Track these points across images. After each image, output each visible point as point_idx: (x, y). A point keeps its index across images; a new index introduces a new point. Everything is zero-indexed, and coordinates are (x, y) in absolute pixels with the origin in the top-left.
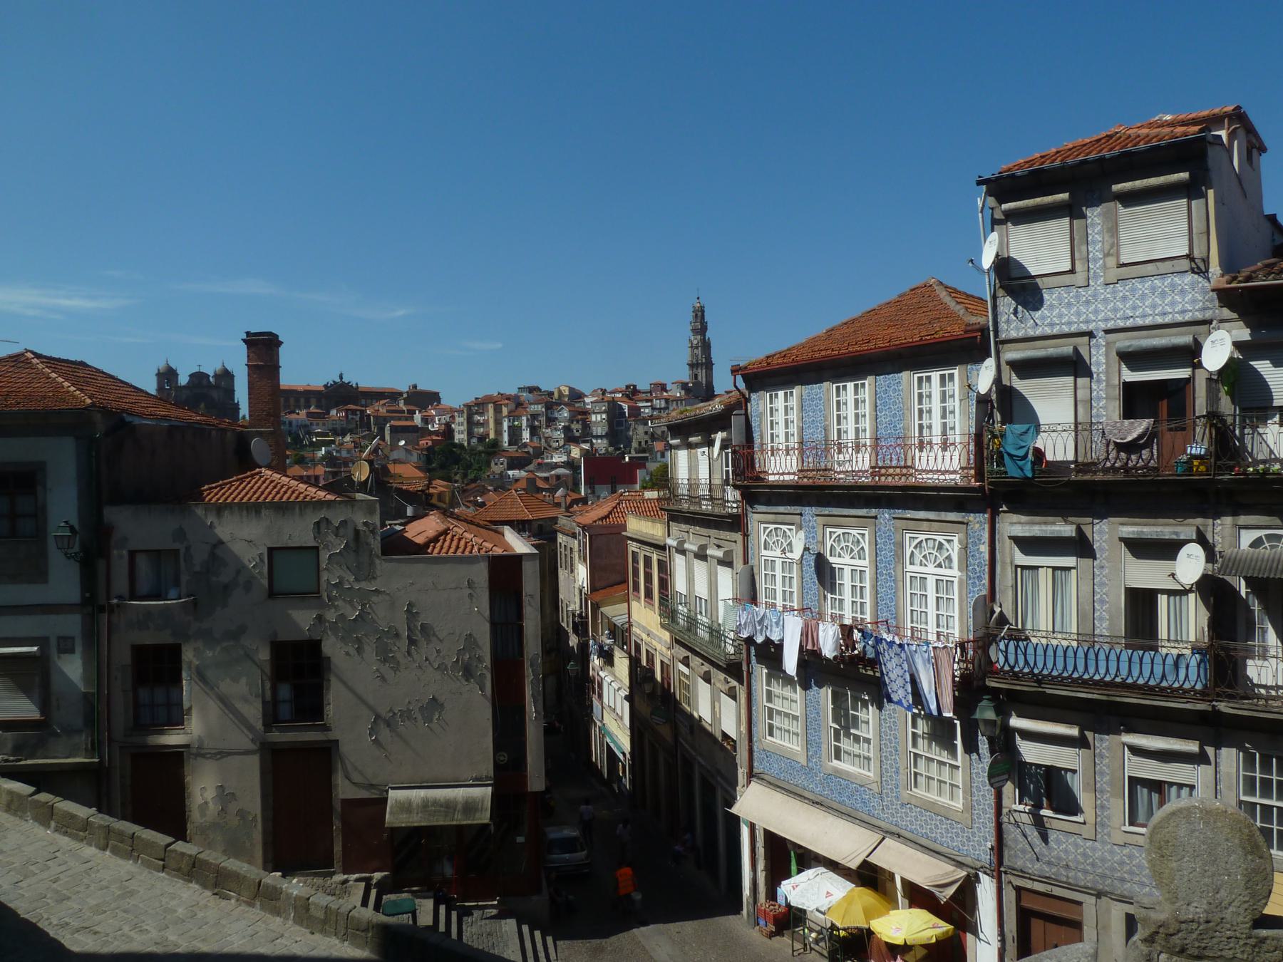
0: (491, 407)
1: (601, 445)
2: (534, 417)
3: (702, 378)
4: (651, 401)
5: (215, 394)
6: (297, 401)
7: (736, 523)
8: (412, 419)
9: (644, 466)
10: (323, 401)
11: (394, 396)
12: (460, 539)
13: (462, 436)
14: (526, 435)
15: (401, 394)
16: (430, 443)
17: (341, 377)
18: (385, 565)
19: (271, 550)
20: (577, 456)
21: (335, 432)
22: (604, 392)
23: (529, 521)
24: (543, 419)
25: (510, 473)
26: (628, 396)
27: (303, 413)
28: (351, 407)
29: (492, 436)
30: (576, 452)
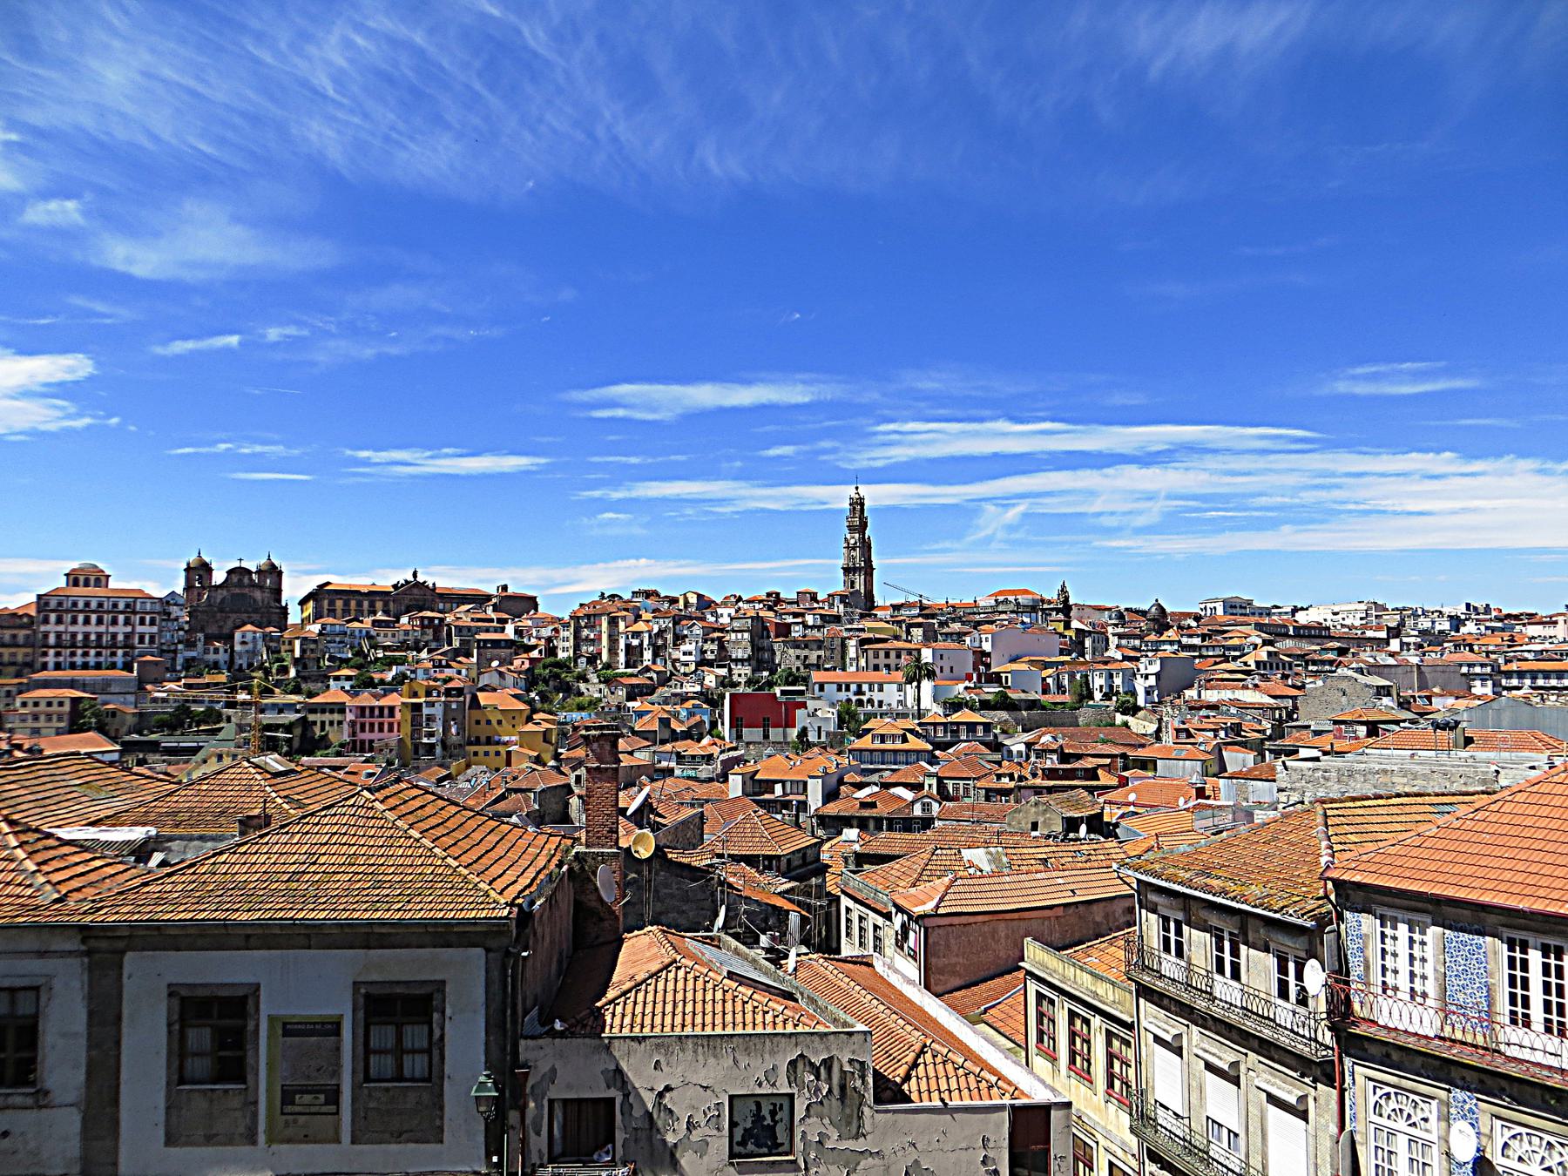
1: (742, 672)
3: (860, 585)
4: (802, 615)
5: (258, 595)
6: (360, 604)
7: (1327, 1073)
8: (503, 630)
9: (804, 705)
11: (480, 599)
12: (944, 1063)
13: (565, 655)
14: (648, 655)
15: (488, 598)
16: (527, 665)
18: (879, 1117)
19: (732, 1098)
20: (713, 685)
21: (404, 646)
22: (740, 599)
23: (778, 857)
24: (670, 637)
25: (630, 704)
26: (770, 609)
27: (368, 621)
29: (605, 657)
30: (710, 681)
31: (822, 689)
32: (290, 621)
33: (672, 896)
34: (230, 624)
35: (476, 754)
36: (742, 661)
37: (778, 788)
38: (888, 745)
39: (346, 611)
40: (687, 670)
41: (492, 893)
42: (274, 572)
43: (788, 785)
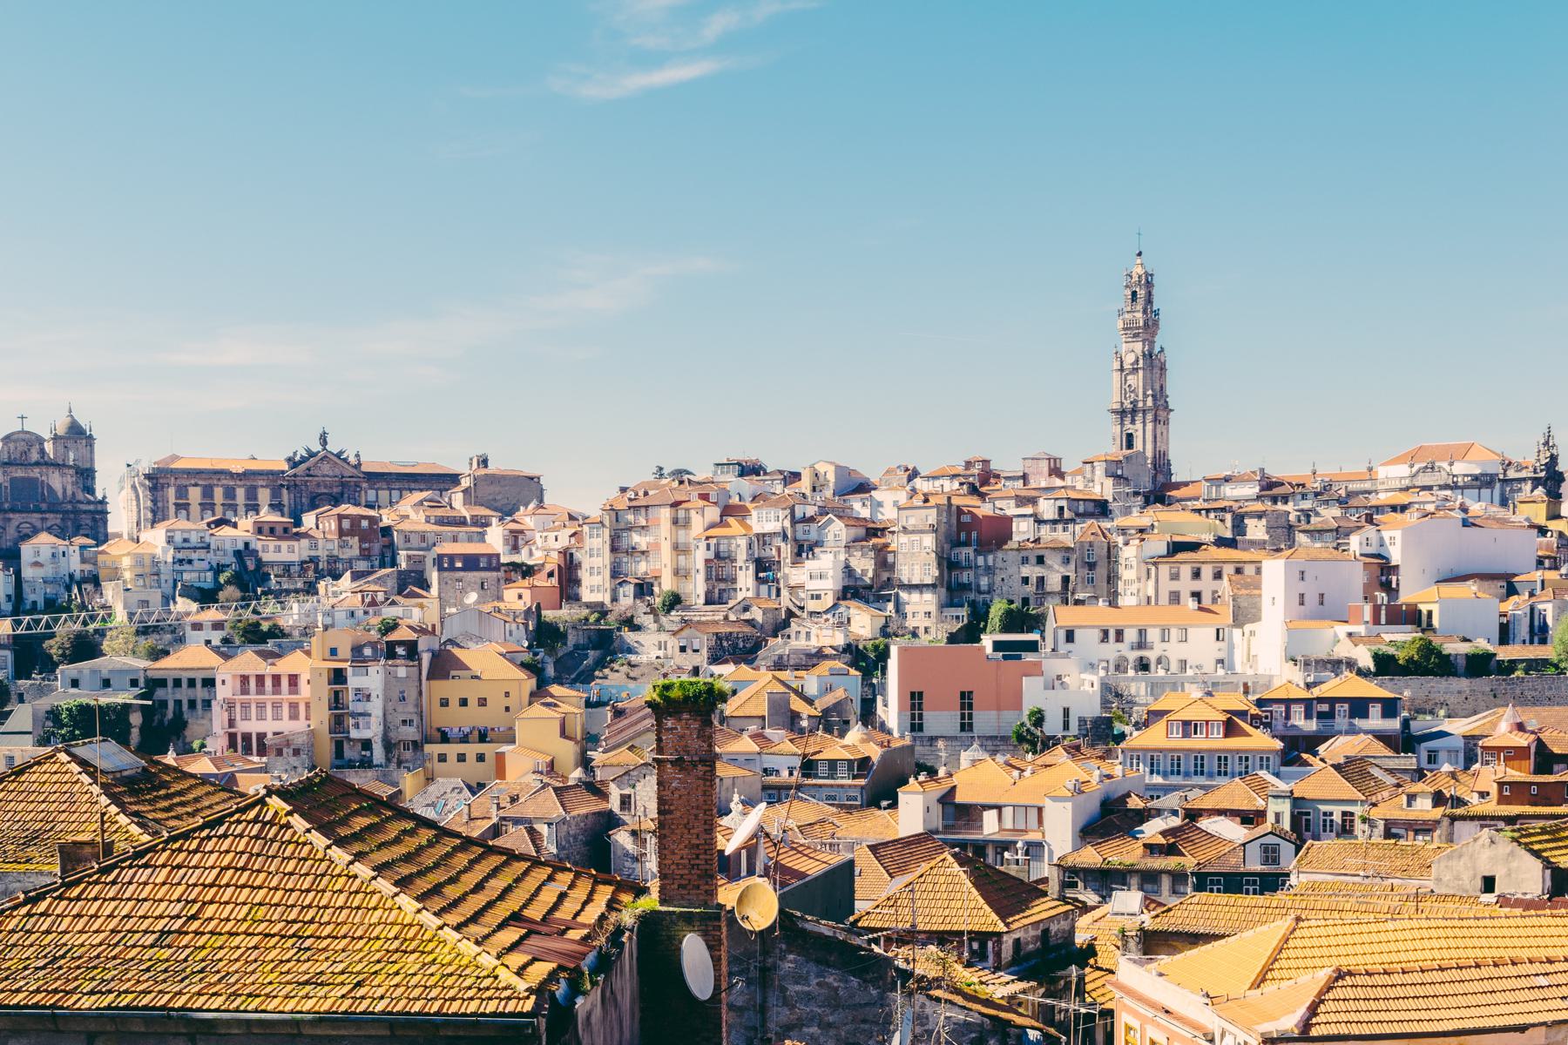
0: (665, 514)
2: (763, 539)
4: (1033, 501)
5: (58, 482)
6: (230, 493)
8: (481, 537)
9: (1035, 670)
10: (285, 496)
13: (597, 580)
15: (454, 479)
17: (324, 440)
22: (913, 474)
23: (999, 935)
26: (973, 490)
27: (246, 524)
28: (348, 509)
31: (1070, 637)
32: (112, 528)
33: (809, 998)
34: (11, 532)
35: (442, 758)
36: (920, 588)
37: (990, 818)
38: (1198, 742)
39: (207, 506)
40: (812, 605)
41: (501, 971)
42: (77, 434)
43: (1008, 812)
